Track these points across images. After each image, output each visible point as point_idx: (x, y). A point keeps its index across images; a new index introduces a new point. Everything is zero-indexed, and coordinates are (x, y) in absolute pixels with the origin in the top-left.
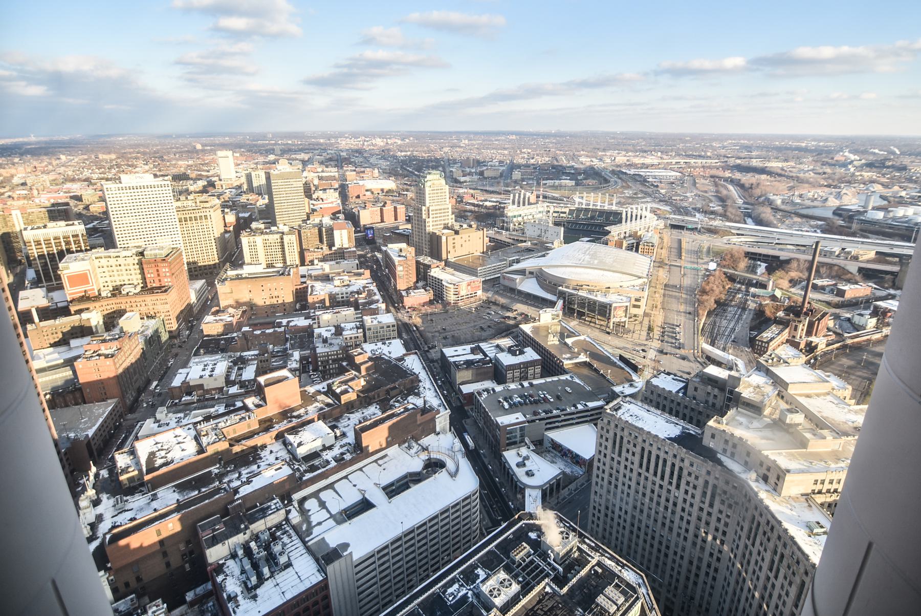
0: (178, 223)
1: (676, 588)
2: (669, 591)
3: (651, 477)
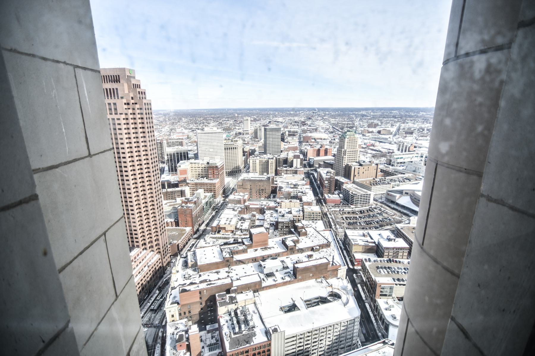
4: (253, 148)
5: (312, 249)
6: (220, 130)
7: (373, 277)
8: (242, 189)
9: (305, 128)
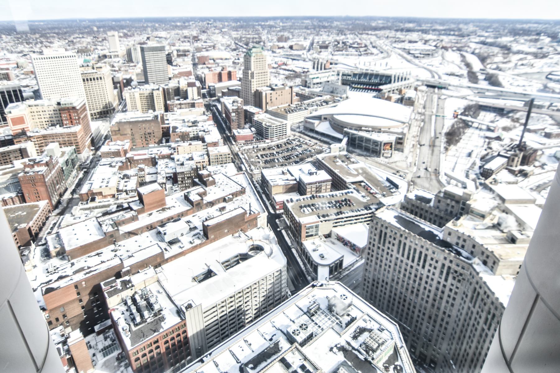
4: (128, 77)
5: (224, 200)
6: (70, 53)
7: (297, 218)
8: (119, 136)
9: (199, 44)
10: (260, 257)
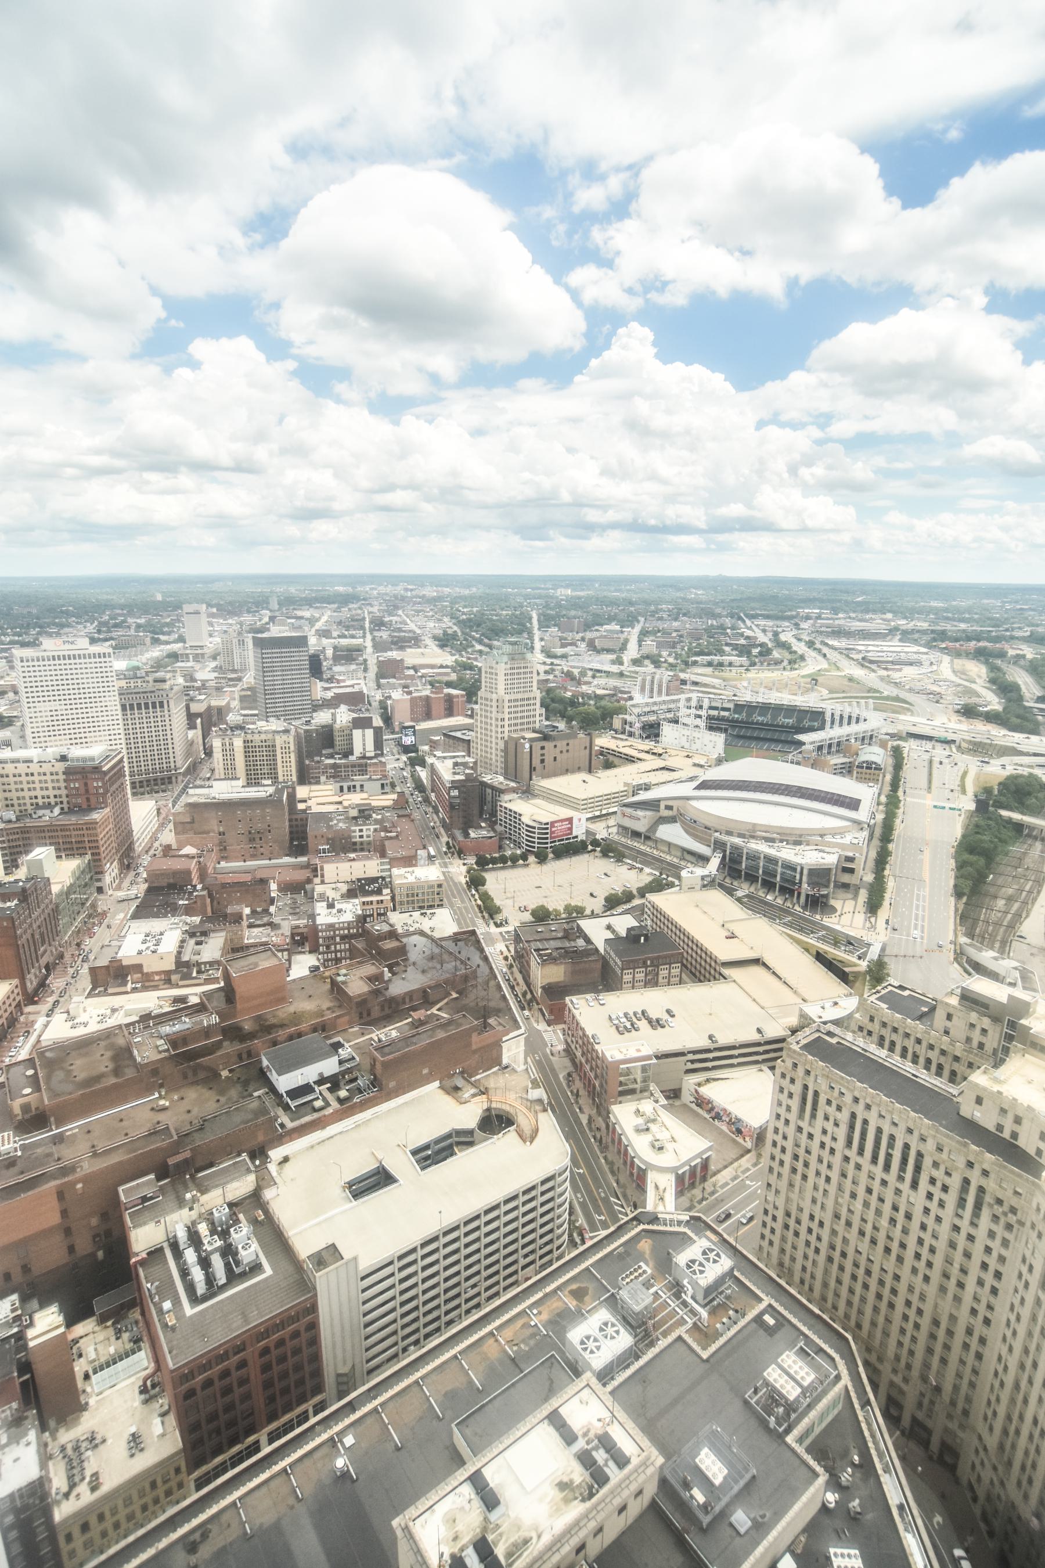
0: (119, 712)
1: (909, 1367)
2: (895, 1371)
3: (865, 1161)
10: (506, 1141)
